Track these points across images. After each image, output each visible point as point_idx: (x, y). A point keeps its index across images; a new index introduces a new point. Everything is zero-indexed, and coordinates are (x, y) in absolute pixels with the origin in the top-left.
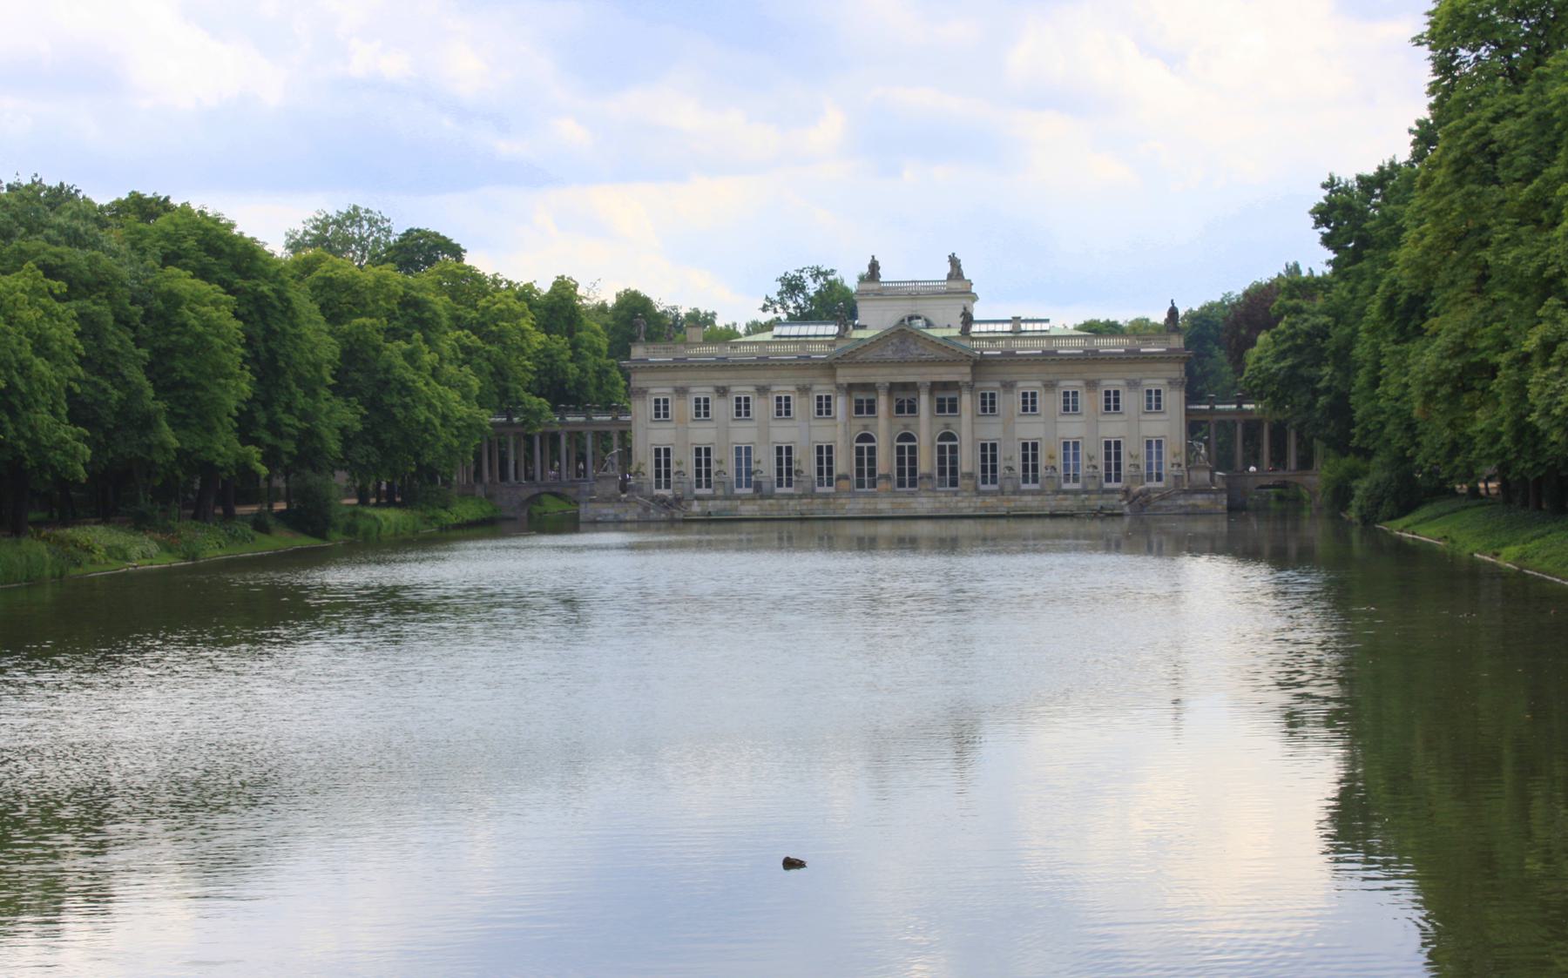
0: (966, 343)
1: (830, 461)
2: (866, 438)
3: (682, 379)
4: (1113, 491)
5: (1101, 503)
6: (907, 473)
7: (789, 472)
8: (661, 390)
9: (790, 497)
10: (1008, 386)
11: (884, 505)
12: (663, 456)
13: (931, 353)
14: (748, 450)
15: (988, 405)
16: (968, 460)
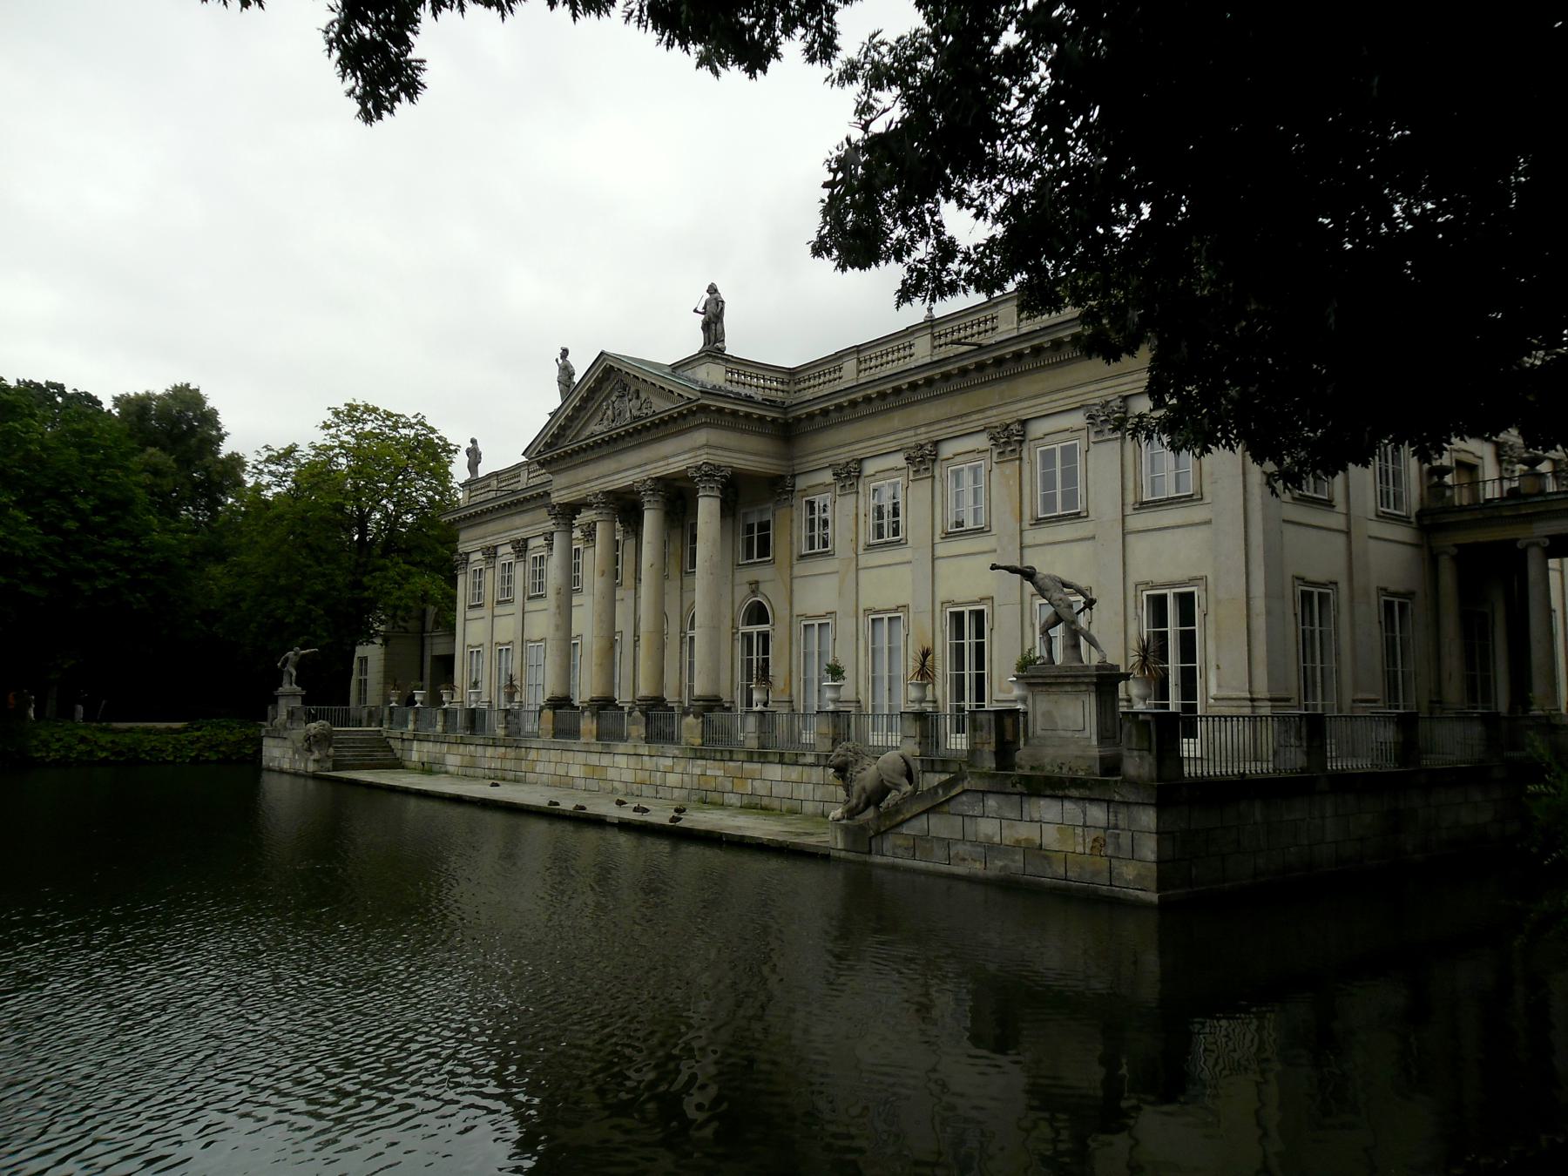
10: (849, 475)
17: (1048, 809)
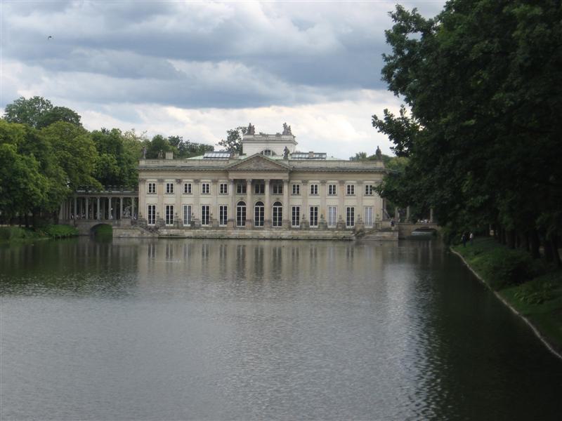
0: (286, 163)
1: (226, 213)
2: (242, 203)
3: (161, 175)
4: (349, 230)
5: (343, 235)
6: (260, 219)
7: (208, 217)
8: (152, 179)
9: (207, 228)
10: (305, 182)
11: (248, 233)
12: (152, 209)
13: (271, 167)
14: (190, 207)
15: (296, 190)
16: (287, 214)
17: (386, 233)
